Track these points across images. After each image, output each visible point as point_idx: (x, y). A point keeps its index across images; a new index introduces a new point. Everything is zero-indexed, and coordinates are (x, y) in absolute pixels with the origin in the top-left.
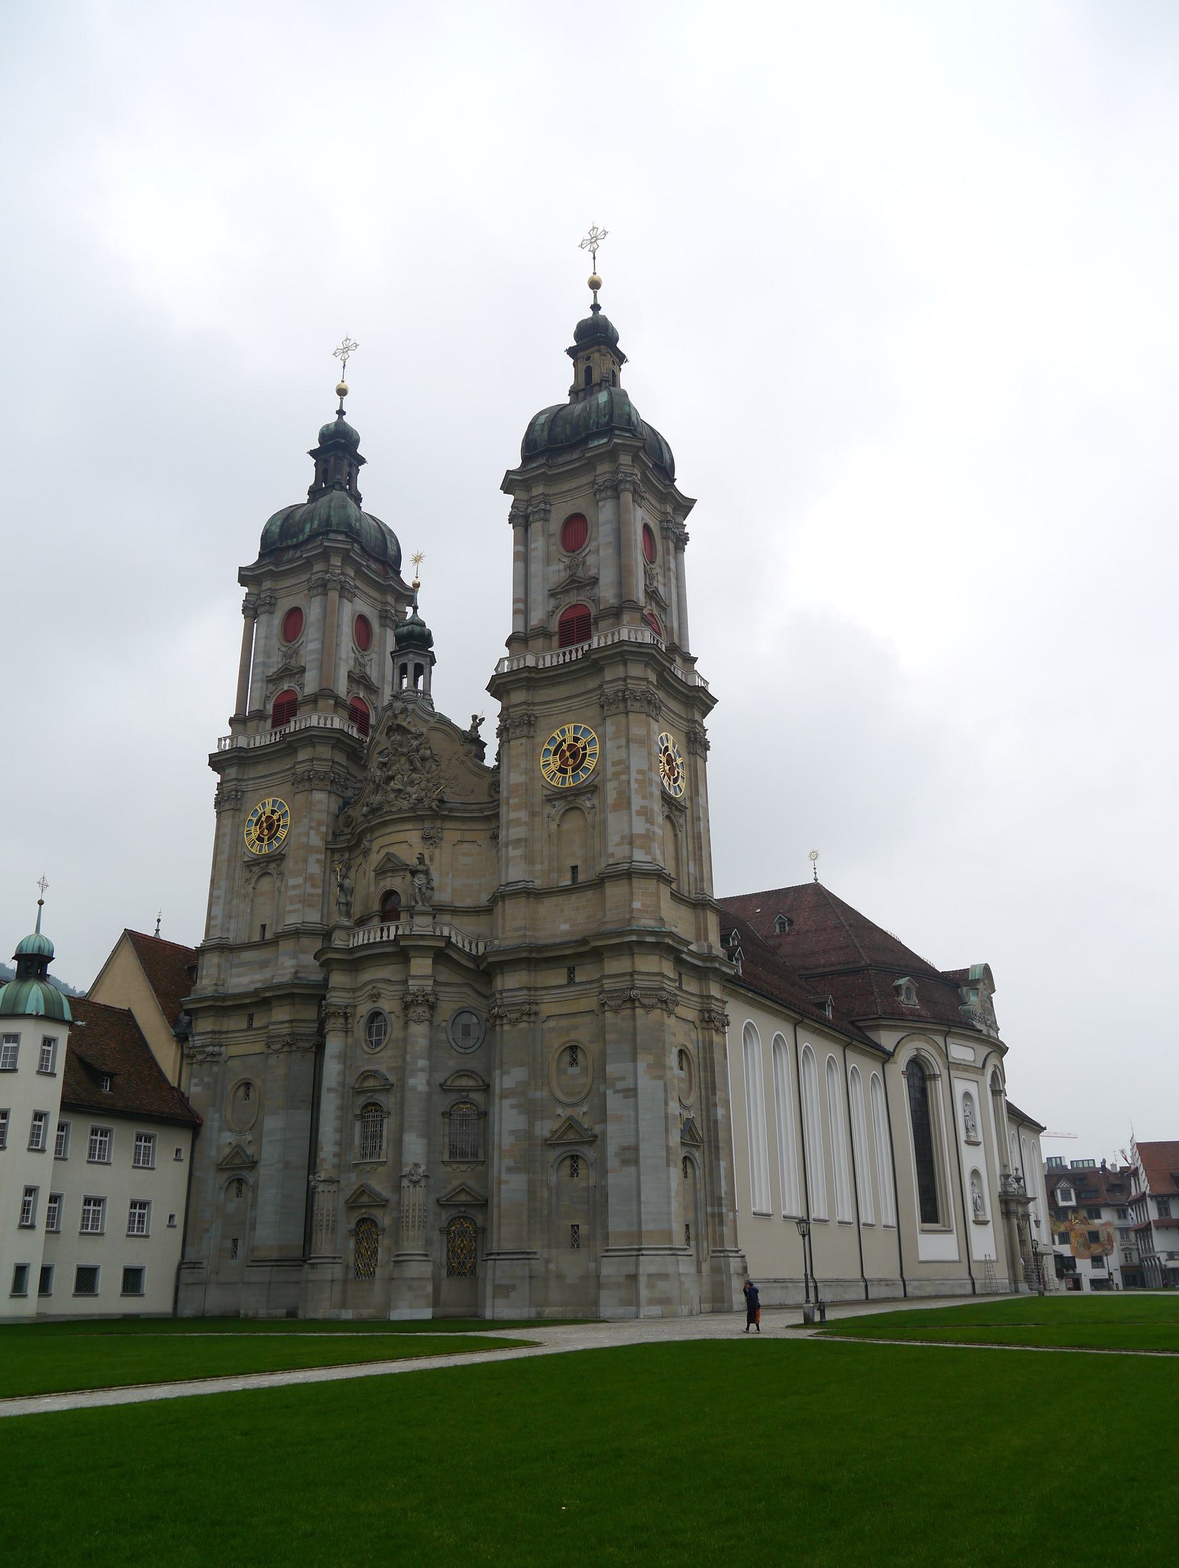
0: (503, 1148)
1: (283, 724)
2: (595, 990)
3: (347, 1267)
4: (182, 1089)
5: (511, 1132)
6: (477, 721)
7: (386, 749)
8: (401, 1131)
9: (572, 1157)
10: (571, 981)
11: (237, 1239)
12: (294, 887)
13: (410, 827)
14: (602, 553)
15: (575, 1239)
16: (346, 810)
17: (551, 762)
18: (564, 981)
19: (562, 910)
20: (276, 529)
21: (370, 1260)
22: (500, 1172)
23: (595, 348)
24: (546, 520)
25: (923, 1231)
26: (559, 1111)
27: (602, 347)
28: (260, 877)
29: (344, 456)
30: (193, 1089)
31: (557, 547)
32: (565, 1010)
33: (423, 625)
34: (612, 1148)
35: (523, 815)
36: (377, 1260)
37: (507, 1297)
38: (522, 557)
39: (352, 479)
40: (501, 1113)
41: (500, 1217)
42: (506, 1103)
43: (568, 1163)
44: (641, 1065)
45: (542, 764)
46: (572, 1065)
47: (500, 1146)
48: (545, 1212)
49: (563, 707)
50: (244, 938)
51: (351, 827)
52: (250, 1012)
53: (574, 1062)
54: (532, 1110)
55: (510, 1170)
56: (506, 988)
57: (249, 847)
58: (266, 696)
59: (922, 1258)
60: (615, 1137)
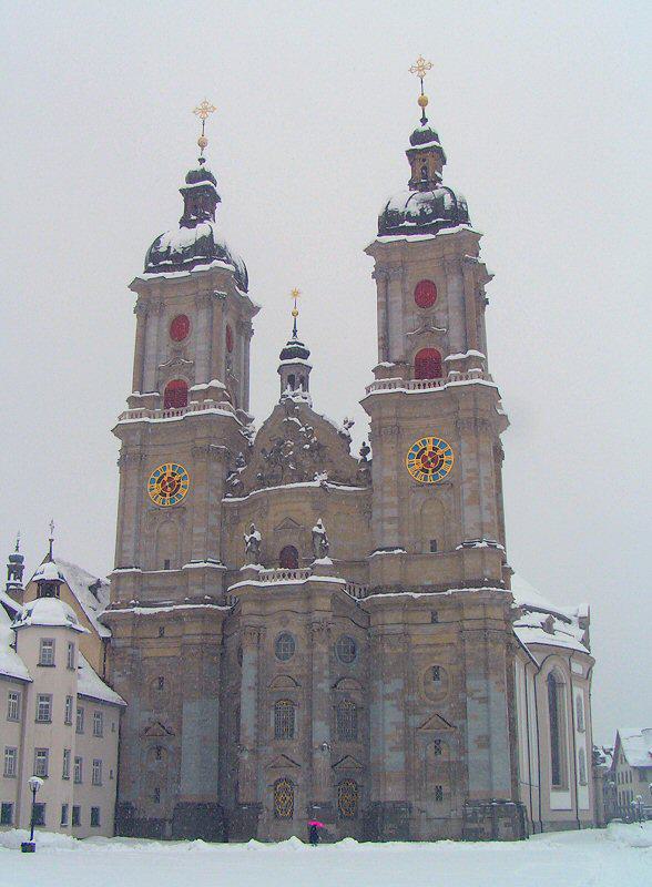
5: (392, 723)
8: (309, 723)
12: (198, 535)
14: (451, 314)
22: (384, 749)
24: (403, 281)
25: (555, 789)
31: (411, 303)
34: (471, 738)
35: (395, 499)
38: (385, 306)
42: (388, 703)
44: (493, 679)
53: (436, 677)
54: (409, 709)
55: (391, 749)
60: (474, 728)
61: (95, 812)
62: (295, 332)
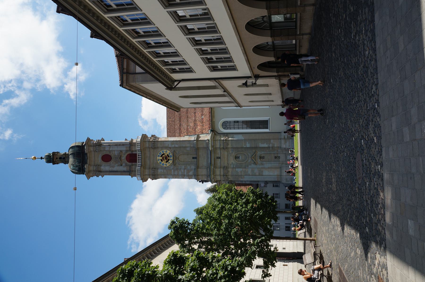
9: (260, 158)
10: (219, 158)
17: (165, 163)
18: (220, 159)
26: (249, 161)
43: (262, 159)
45: (165, 166)
56: (220, 174)
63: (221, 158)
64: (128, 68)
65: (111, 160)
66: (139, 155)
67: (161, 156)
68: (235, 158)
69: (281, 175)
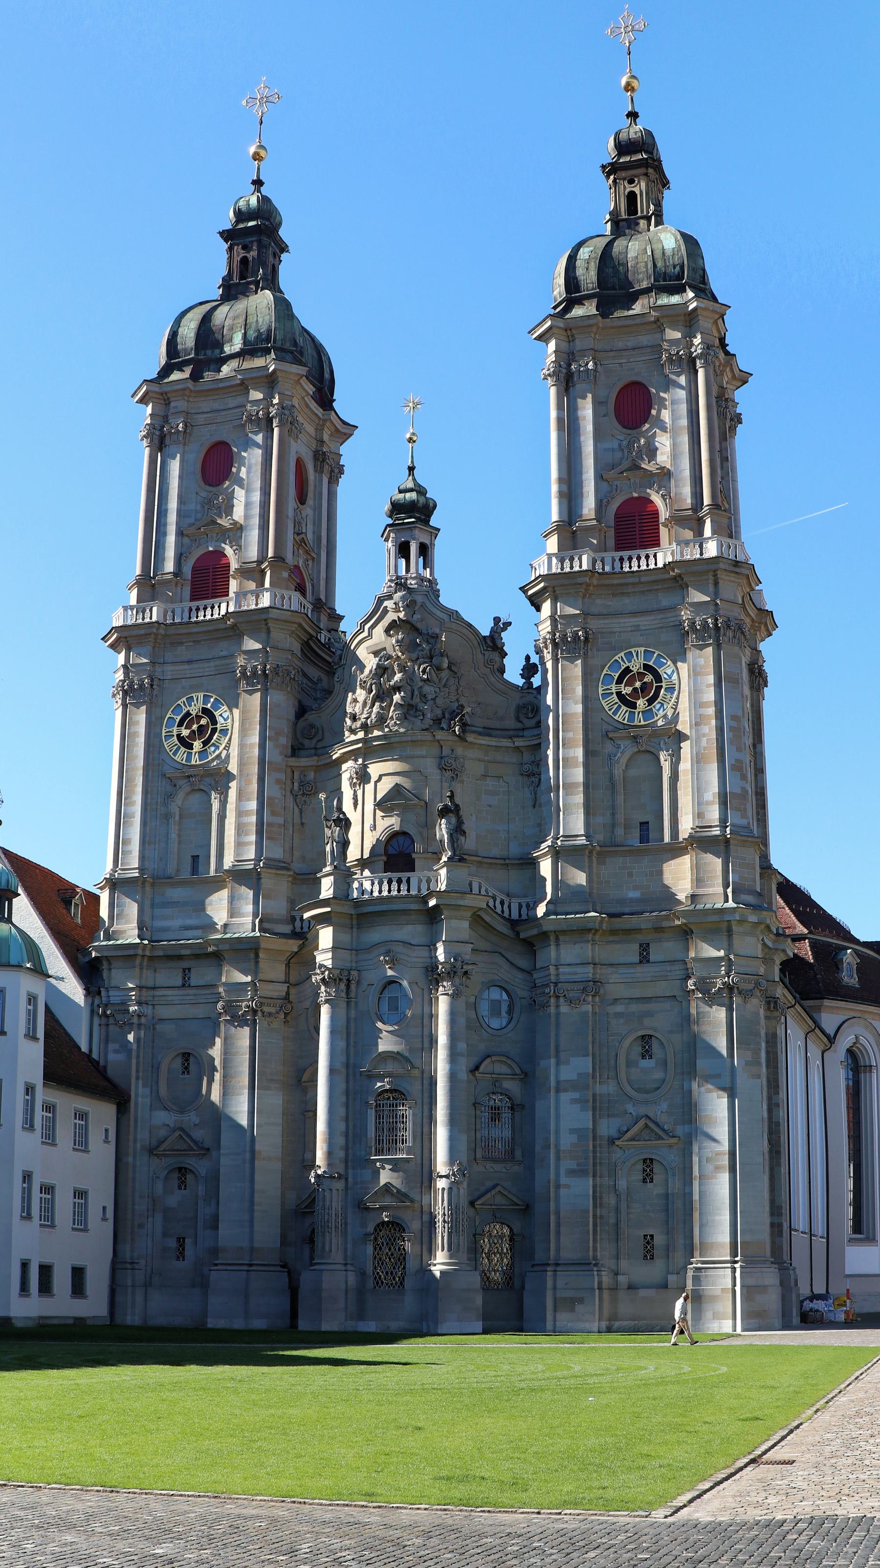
0: (562, 1148)
1: (207, 598)
2: (678, 972)
3: (363, 1274)
4: (95, 1056)
5: (572, 1131)
6: (500, 626)
7: (385, 649)
9: (645, 1161)
10: (644, 959)
11: (184, 1239)
13: (424, 753)
15: (649, 1251)
16: (306, 716)
17: (614, 691)
18: (636, 959)
19: (630, 875)
20: (188, 331)
21: (394, 1268)
22: (558, 1175)
23: (642, 170)
26: (630, 1108)
27: (650, 170)
28: (188, 794)
29: (270, 244)
30: (111, 1057)
32: (637, 993)
33: (420, 490)
36: (404, 1268)
37: (573, 1310)
39: (275, 271)
40: (557, 1108)
41: (558, 1225)
42: (565, 1097)
43: (640, 1166)
45: (600, 692)
46: (643, 1057)
47: (557, 1146)
48: (612, 1221)
49: (627, 625)
50: (171, 870)
51: (314, 741)
52: (185, 964)
53: (647, 1053)
55: (571, 1173)
56: (562, 962)
57: (171, 754)
58: (181, 554)
59: (847, 1273)
61: (78, 1273)
62: (411, 469)
63: (646, 969)
64: (234, 548)
65: (625, 427)
66: (652, 557)
67: (646, 667)
68: (643, 1037)
69: (558, 1269)
